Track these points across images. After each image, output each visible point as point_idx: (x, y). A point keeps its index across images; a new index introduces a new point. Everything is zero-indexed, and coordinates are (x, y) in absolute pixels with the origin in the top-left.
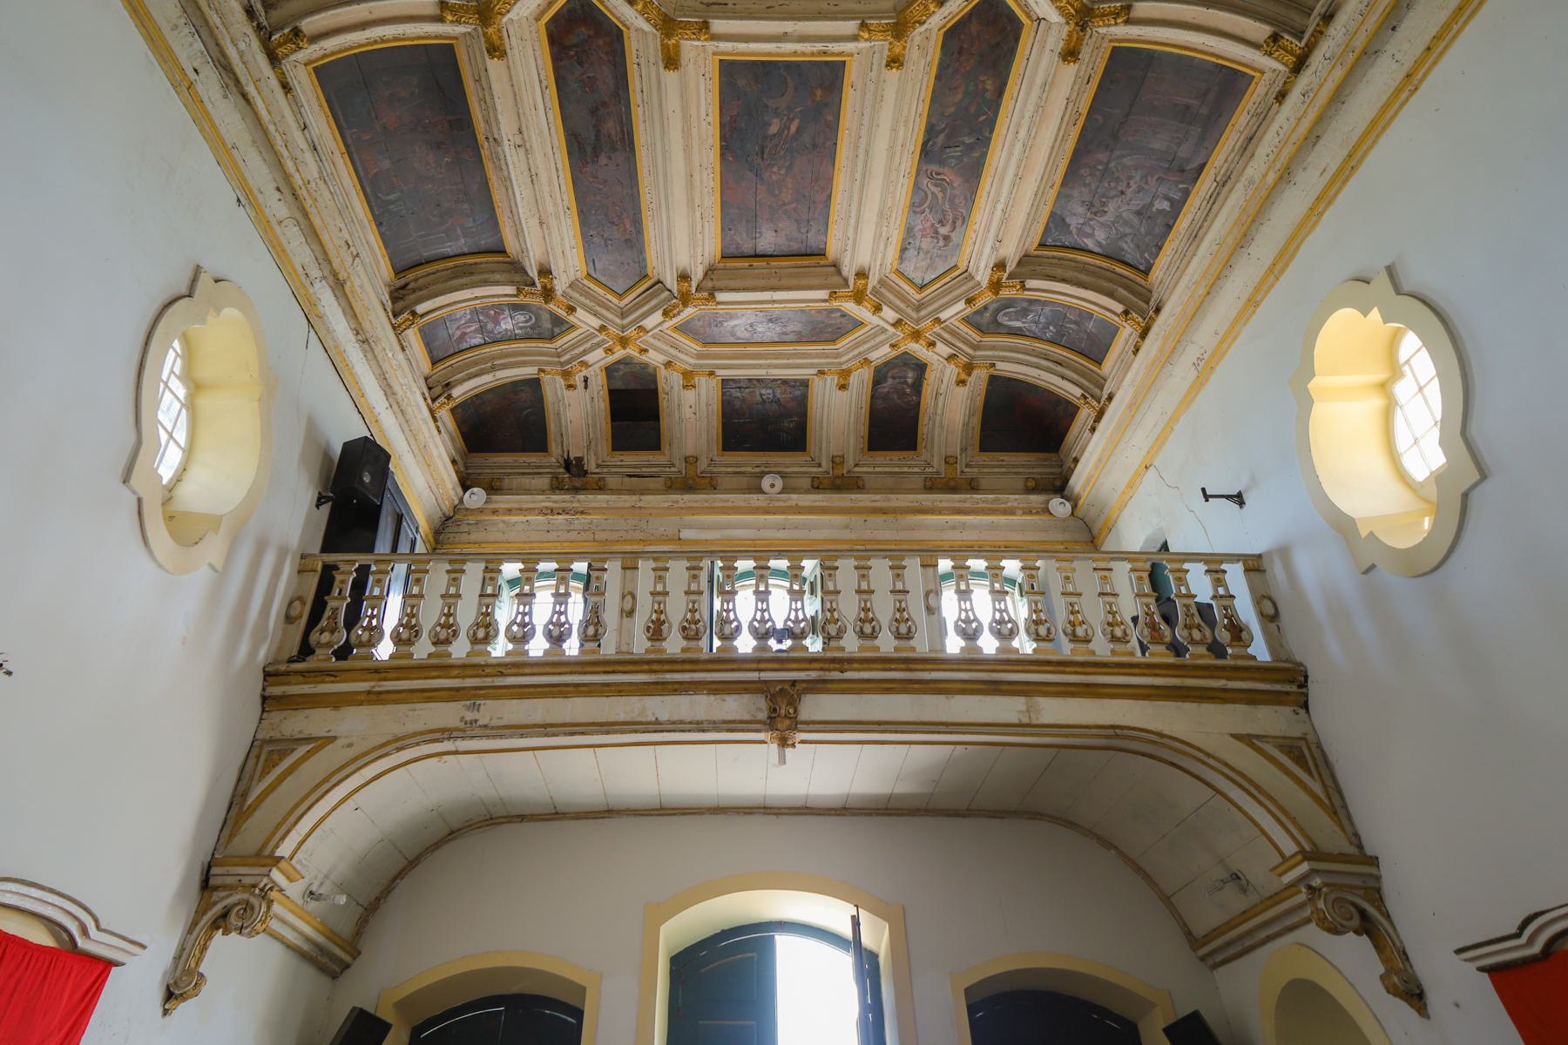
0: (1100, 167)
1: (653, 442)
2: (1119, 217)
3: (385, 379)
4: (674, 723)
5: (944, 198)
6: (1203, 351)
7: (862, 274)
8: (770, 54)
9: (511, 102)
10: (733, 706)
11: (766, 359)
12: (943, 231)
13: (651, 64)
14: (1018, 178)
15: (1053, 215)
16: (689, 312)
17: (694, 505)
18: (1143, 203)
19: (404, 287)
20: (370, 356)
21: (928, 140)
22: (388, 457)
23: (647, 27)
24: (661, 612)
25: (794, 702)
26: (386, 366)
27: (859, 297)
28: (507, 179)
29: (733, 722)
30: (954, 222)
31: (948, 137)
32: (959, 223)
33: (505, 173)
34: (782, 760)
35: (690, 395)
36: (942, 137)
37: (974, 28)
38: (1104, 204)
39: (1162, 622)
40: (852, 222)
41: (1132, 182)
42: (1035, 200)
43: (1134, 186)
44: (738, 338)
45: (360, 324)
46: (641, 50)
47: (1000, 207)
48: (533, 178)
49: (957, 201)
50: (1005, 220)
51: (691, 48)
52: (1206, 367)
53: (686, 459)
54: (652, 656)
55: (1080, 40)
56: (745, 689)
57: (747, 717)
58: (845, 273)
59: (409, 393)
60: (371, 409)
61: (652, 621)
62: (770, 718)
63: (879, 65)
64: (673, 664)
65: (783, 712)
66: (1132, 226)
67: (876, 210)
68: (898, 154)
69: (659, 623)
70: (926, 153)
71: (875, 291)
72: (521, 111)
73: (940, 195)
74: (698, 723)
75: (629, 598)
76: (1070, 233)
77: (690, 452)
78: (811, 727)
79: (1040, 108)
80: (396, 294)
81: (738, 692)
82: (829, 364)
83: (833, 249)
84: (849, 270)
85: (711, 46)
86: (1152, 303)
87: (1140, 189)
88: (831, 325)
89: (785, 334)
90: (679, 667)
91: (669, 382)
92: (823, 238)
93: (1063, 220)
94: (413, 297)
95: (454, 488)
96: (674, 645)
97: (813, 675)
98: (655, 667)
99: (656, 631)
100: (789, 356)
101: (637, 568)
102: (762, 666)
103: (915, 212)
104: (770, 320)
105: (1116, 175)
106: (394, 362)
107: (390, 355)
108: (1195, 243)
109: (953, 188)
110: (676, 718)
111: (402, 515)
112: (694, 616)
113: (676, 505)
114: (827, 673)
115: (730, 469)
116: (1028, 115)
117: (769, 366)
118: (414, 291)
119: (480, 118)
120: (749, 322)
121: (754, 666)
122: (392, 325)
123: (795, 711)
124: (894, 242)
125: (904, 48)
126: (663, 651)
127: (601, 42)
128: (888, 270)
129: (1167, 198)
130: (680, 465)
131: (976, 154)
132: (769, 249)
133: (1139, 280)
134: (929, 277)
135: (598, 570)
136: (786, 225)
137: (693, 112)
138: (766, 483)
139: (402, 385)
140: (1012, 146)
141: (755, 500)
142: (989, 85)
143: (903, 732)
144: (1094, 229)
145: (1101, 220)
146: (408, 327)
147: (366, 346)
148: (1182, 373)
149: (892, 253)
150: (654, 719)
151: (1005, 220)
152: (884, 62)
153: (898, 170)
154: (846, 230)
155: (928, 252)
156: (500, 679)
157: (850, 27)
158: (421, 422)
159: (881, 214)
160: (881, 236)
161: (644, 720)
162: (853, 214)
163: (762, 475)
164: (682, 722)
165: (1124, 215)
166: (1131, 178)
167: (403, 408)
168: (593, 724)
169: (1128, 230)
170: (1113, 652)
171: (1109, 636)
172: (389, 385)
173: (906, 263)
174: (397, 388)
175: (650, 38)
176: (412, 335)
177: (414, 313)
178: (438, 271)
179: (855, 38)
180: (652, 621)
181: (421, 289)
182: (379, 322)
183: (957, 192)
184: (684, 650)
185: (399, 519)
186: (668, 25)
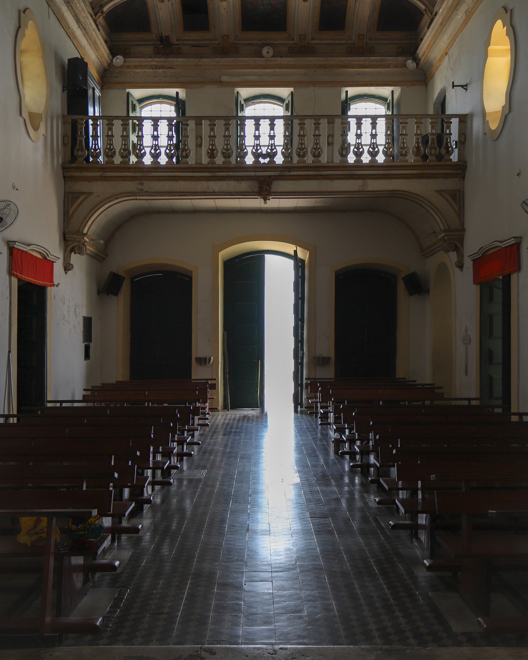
3: (77, 17)
4: (221, 192)
10: (244, 186)
20: (70, 8)
24: (213, 145)
25: (269, 185)
26: (77, 12)
29: (245, 192)
54: (210, 166)
57: (250, 190)
59: (86, 19)
61: (210, 149)
64: (220, 169)
65: (264, 189)
69: (213, 150)
74: (230, 192)
75: (199, 139)
95: (108, 57)
96: (219, 160)
97: (277, 173)
99: (212, 154)
102: (256, 170)
106: (80, 8)
107: (78, 5)
111: (94, 88)
112: (227, 147)
114: (283, 172)
123: (270, 188)
126: (215, 163)
139: (83, 17)
147: (68, 4)
150: (212, 191)
158: (92, 31)
161: (208, 191)
164: (224, 192)
167: (85, 27)
171: (400, 154)
172: (79, 19)
180: (210, 149)
184: (224, 162)
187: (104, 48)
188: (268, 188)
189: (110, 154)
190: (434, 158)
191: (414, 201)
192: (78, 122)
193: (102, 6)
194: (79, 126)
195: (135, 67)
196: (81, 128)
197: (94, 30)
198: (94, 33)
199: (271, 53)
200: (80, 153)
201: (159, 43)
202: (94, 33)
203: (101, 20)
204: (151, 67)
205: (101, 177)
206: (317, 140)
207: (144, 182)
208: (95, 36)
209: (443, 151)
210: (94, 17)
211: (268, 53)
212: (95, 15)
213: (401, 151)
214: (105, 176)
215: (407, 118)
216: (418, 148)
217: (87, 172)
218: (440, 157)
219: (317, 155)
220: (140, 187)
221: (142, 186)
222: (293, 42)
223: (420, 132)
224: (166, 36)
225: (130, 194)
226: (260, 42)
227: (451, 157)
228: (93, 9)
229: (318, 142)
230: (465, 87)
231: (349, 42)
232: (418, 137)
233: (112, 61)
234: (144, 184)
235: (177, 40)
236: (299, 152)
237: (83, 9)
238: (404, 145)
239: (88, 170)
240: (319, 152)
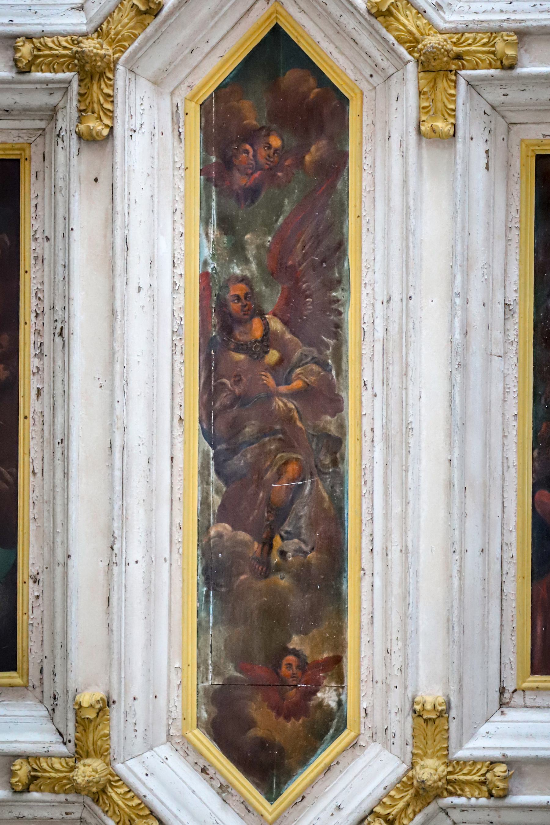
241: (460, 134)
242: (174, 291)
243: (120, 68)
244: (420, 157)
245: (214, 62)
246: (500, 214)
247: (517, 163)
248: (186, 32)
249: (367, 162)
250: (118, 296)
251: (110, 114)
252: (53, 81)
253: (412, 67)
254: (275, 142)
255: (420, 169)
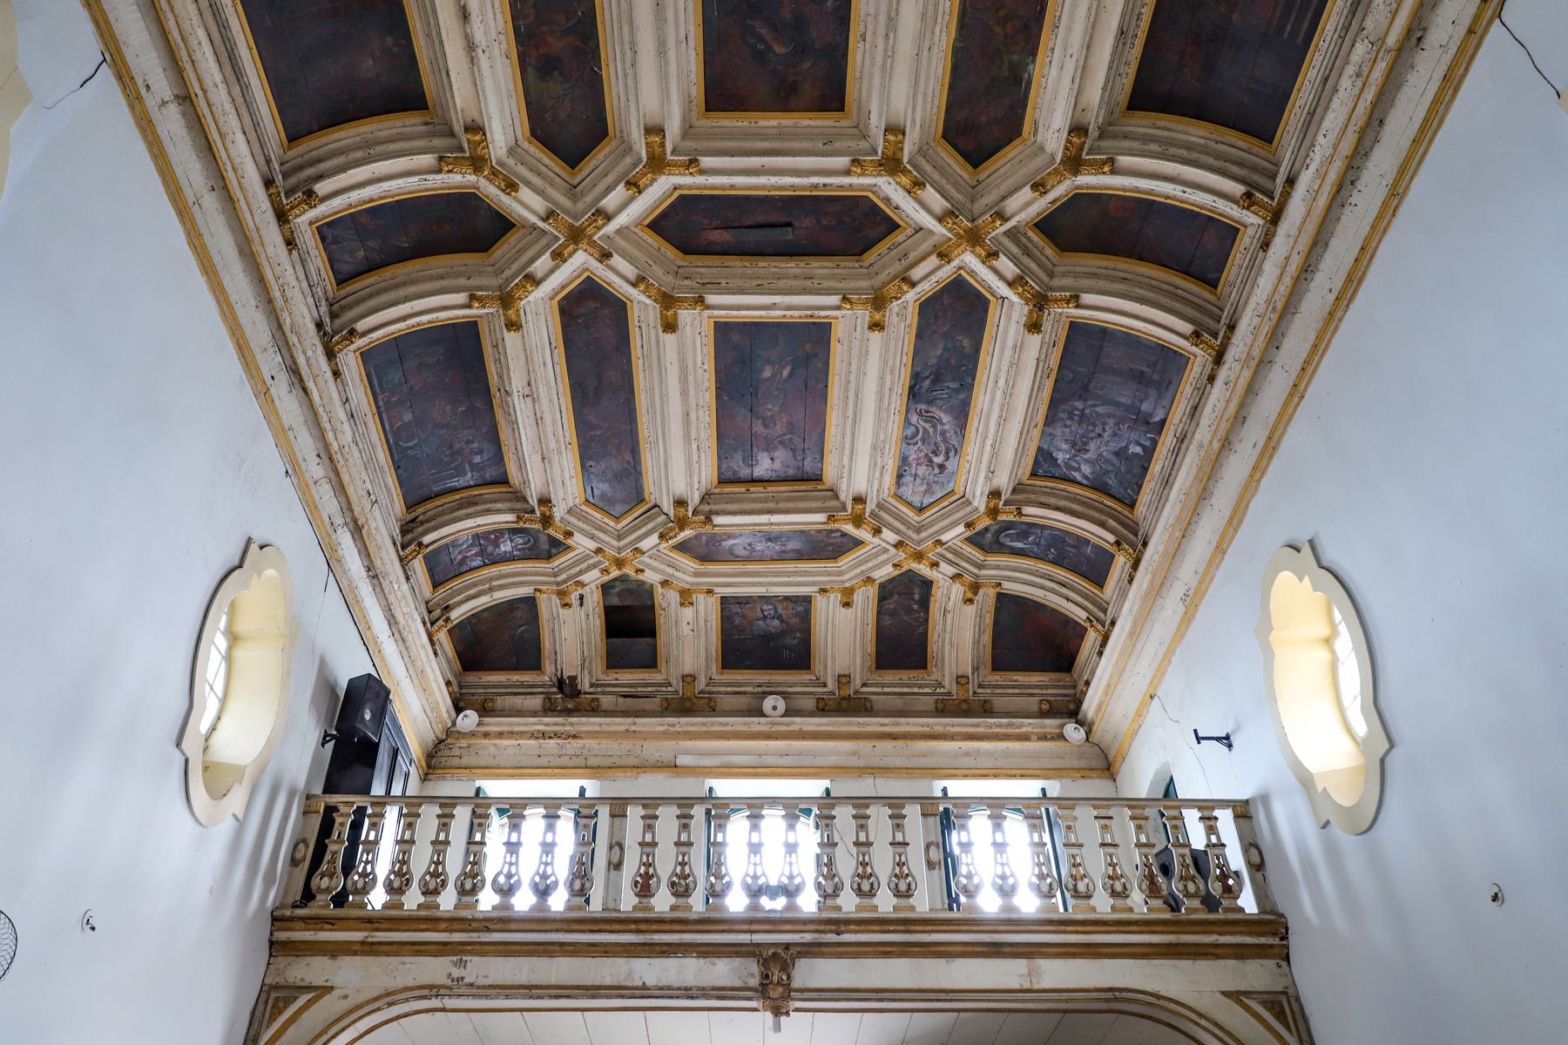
0: (1077, 413)
1: (651, 663)
2: (1101, 455)
5: (935, 431)
6: (1186, 588)
7: (859, 500)
8: (761, 317)
9: (523, 361)
10: (722, 971)
11: (766, 576)
12: (938, 460)
13: (651, 327)
14: (1003, 420)
15: (1040, 449)
16: (687, 533)
17: (691, 729)
18: (1119, 446)
19: (413, 521)
20: (378, 589)
21: (915, 385)
22: (388, 692)
23: (648, 301)
24: (650, 865)
25: (786, 967)
26: (391, 598)
27: (858, 521)
28: (514, 424)
30: (947, 453)
31: (934, 382)
32: (952, 454)
33: (513, 418)
34: (777, 1028)
35: (688, 612)
36: (927, 382)
37: (947, 300)
38: (1085, 444)
39: (1160, 874)
40: (847, 452)
41: (1107, 428)
42: (1020, 438)
43: (1109, 431)
44: (737, 556)
45: (371, 561)
46: (642, 316)
47: (989, 442)
48: (538, 421)
49: (948, 435)
50: (995, 454)
51: (686, 316)
52: (1192, 601)
53: (684, 677)
54: (640, 915)
55: (1040, 318)
56: (737, 953)
57: (738, 983)
58: (842, 497)
60: (375, 639)
61: (641, 875)
62: (762, 984)
63: (862, 327)
64: (661, 923)
65: (775, 978)
66: (1113, 465)
67: (869, 443)
68: (887, 396)
69: (647, 877)
70: (914, 393)
71: (873, 514)
72: (531, 369)
73: (931, 430)
74: (686, 989)
75: (616, 849)
76: (1059, 466)
77: (688, 670)
78: (806, 995)
79: (1015, 365)
80: (406, 527)
81: (729, 955)
82: (830, 582)
83: (830, 473)
84: (846, 495)
85: (707, 313)
86: (1139, 536)
87: (1115, 435)
88: (831, 544)
89: (784, 552)
90: (668, 927)
91: (666, 600)
92: (820, 465)
93: (1051, 454)
94: (420, 529)
96: (662, 902)
97: (808, 937)
98: (643, 927)
99: (644, 887)
100: (789, 574)
101: (626, 816)
102: (754, 927)
103: (908, 444)
104: (769, 540)
105: (1092, 420)
106: (399, 594)
107: (396, 587)
108: (1167, 488)
109: (943, 424)
110: (664, 983)
112: (683, 870)
113: (671, 729)
114: (823, 935)
115: (729, 689)
116: (1004, 369)
117: (770, 584)
118: (422, 523)
119: (494, 373)
120: (748, 541)
121: (746, 927)
122: (399, 556)
123: (789, 978)
124: (890, 470)
125: (884, 316)
126: (651, 909)
127: (606, 311)
128: (886, 495)
129: (1139, 444)
130: (677, 684)
131: (962, 396)
132: (766, 476)
133: (1126, 513)
134: (926, 502)
135: (586, 817)
136: (781, 454)
137: (690, 363)
138: (768, 703)
139: (404, 614)
140: (993, 393)
141: (756, 724)
142: (966, 343)
143: (901, 1000)
144: (1080, 464)
145: (1085, 457)
146: (414, 558)
148: (1171, 608)
149: (889, 479)
151: (995, 454)
152: (867, 326)
153: (888, 410)
154: (841, 460)
155: (923, 479)
156: (487, 934)
157: (834, 300)
159: (874, 447)
160: (876, 464)
162: (847, 446)
163: (766, 694)
164: (669, 988)
165: (1105, 454)
166: (1104, 424)
168: (578, 987)
169: (1110, 468)
170: (1113, 908)
171: (1110, 891)
173: (903, 488)
174: (400, 618)
175: (651, 308)
176: (418, 565)
177: (420, 545)
178: (445, 504)
179: (838, 308)
180: (641, 875)
181: (428, 521)
182: (388, 557)
183: (947, 427)
184: (673, 908)
185: (395, 754)
186: (667, 301)
187: (440, 690)
188: (784, 977)
189: (396, 885)
190: (1196, 903)
191: (1170, 1025)
192: (338, 811)
193: (447, 609)
194: (338, 820)
195: (500, 735)
196: (342, 824)
197: (423, 646)
198: (422, 653)
199: (781, 705)
200: (325, 882)
201: (555, 690)
202: (422, 653)
203: (442, 636)
204: (533, 736)
205: (363, 943)
206: (900, 856)
207: (469, 958)
208: (424, 660)
209: (1215, 888)
210: (429, 625)
211: (775, 708)
212: (432, 624)
213: (1112, 885)
214: (374, 940)
215: (1108, 807)
216: (1151, 878)
217: (331, 930)
218: (1210, 903)
219: (903, 894)
220: (456, 973)
221: (462, 968)
222: (825, 690)
223: (1147, 838)
224: (569, 677)
225: (426, 992)
226: (760, 689)
227: (1240, 902)
228: (430, 612)
229: (903, 859)
230: (1226, 740)
231: (938, 690)
232: (1145, 850)
233: (454, 723)
234: (468, 964)
235: (592, 685)
236: (859, 885)
237: (404, 597)
238: (1114, 870)
239: (333, 925)
240: (909, 884)
241: (882, 132)
242: (1053, 49)
243: (1058, 161)
244: (905, 121)
245: (1010, 155)
246: (865, 86)
247: (855, 109)
248: (1021, 172)
249: (935, 110)
250: (1083, 56)
251: (1068, 141)
252: (1097, 154)
253: (905, 160)
254: (984, 119)
255: (905, 115)
